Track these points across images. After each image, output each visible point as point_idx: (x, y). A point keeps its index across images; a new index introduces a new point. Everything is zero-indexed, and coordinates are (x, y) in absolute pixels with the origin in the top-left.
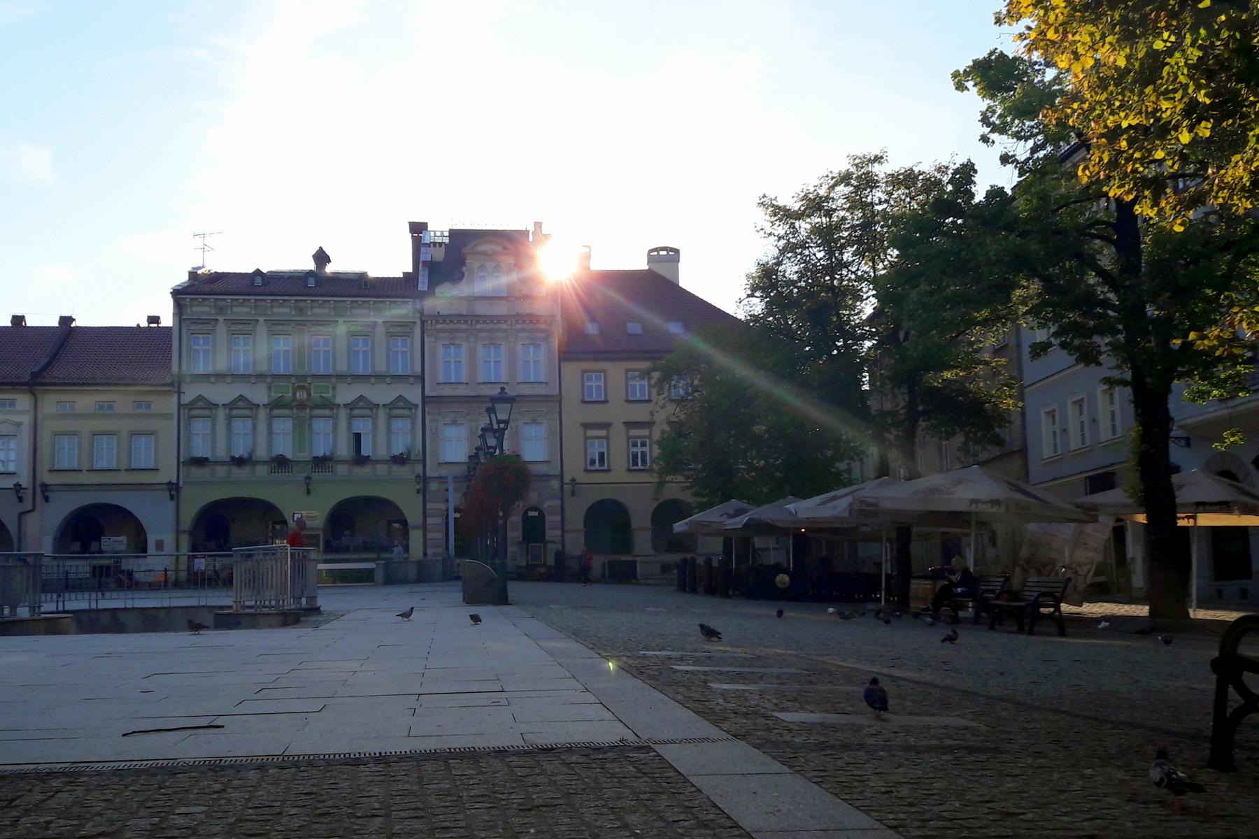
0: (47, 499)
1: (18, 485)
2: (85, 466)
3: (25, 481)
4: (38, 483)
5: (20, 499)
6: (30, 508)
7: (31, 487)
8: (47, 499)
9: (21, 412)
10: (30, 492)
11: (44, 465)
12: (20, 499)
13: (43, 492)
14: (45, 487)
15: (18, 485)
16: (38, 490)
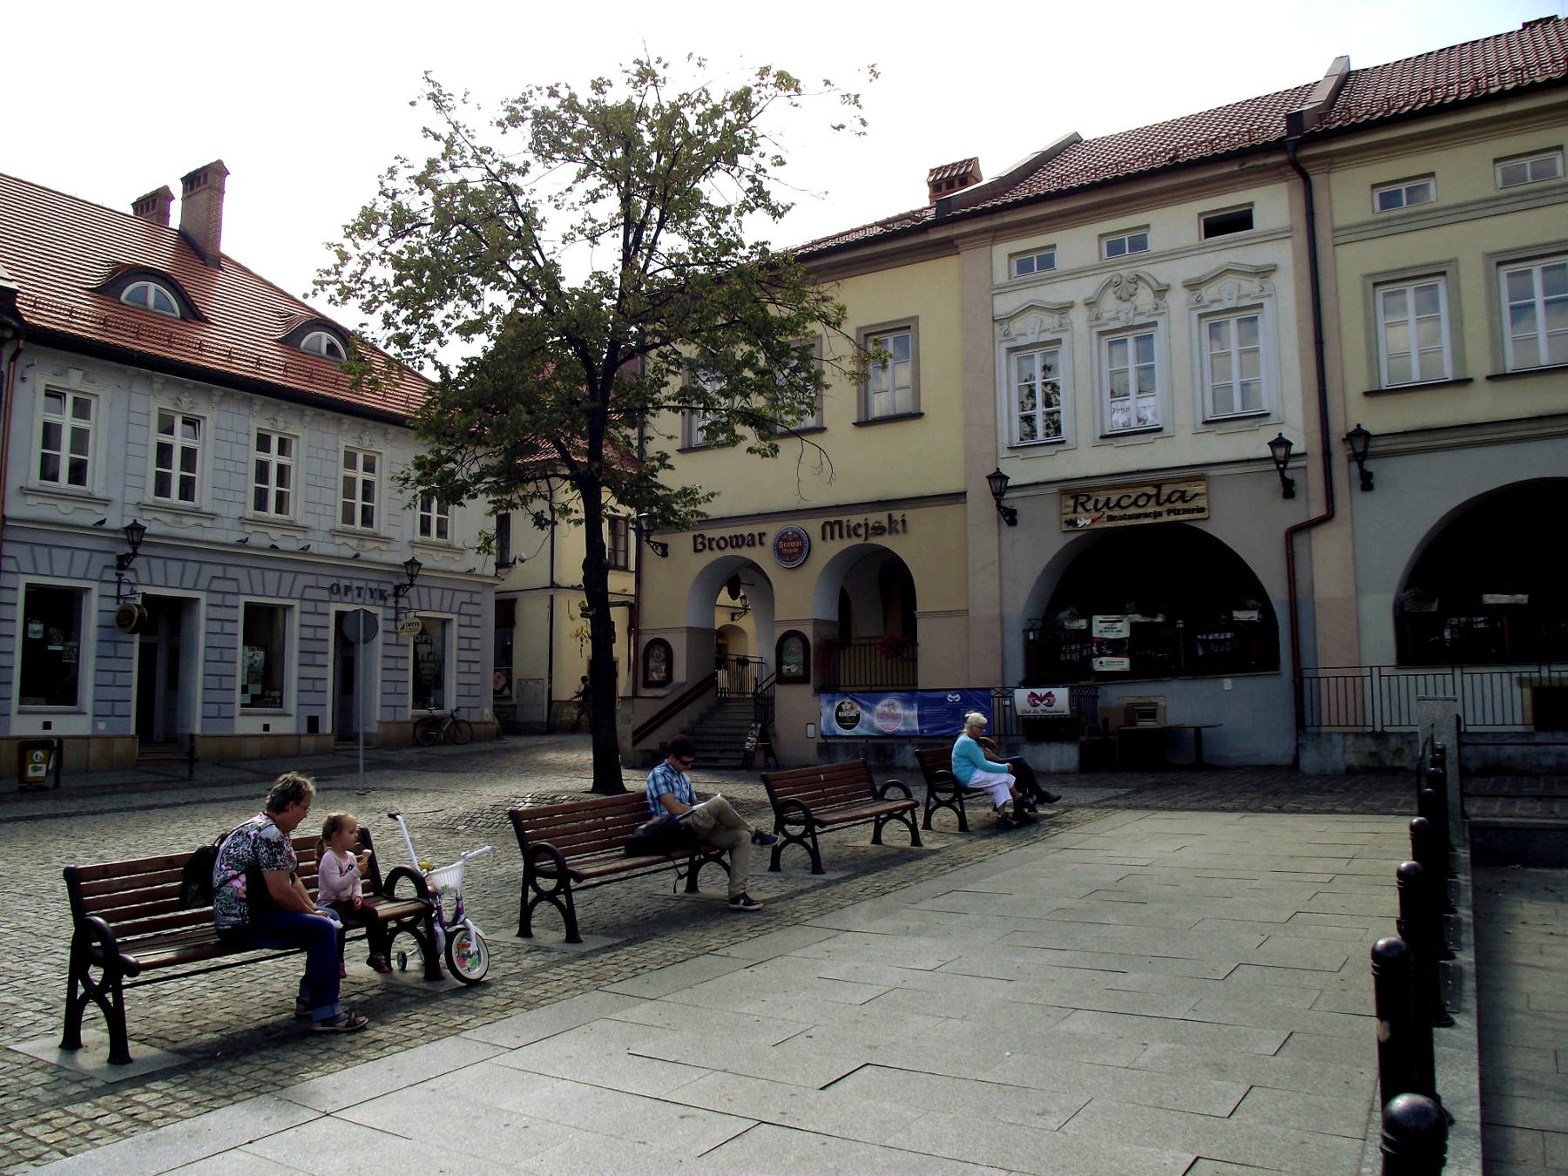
0: (1367, 483)
1: (1280, 442)
2: (1479, 367)
3: (1301, 436)
4: (1336, 440)
5: (1288, 490)
6: (1318, 510)
7: (1317, 450)
8: (1367, 483)
9: (1272, 236)
10: (1315, 466)
11: (1351, 376)
12: (1288, 490)
13: (1359, 458)
14: (1358, 435)
15: (1280, 442)
16: (1340, 454)
